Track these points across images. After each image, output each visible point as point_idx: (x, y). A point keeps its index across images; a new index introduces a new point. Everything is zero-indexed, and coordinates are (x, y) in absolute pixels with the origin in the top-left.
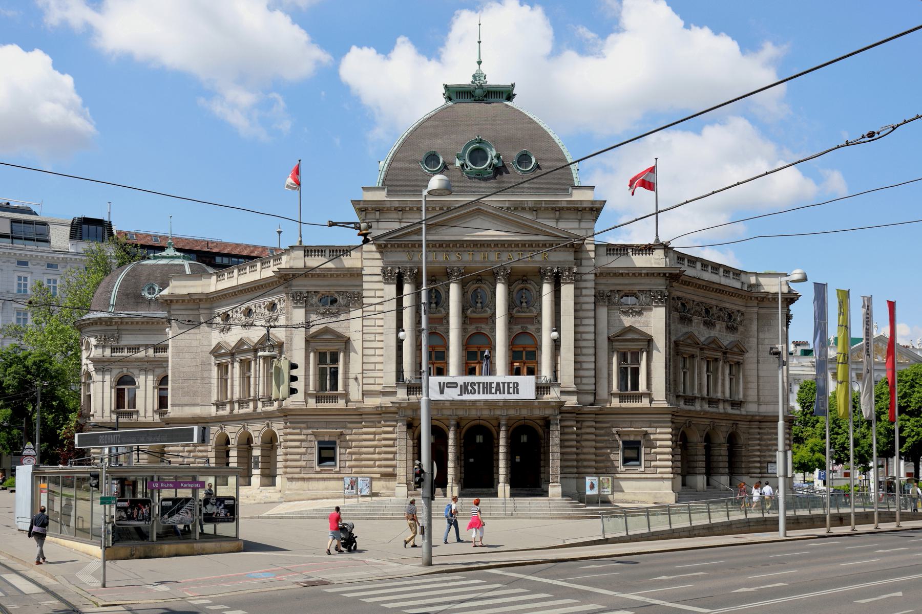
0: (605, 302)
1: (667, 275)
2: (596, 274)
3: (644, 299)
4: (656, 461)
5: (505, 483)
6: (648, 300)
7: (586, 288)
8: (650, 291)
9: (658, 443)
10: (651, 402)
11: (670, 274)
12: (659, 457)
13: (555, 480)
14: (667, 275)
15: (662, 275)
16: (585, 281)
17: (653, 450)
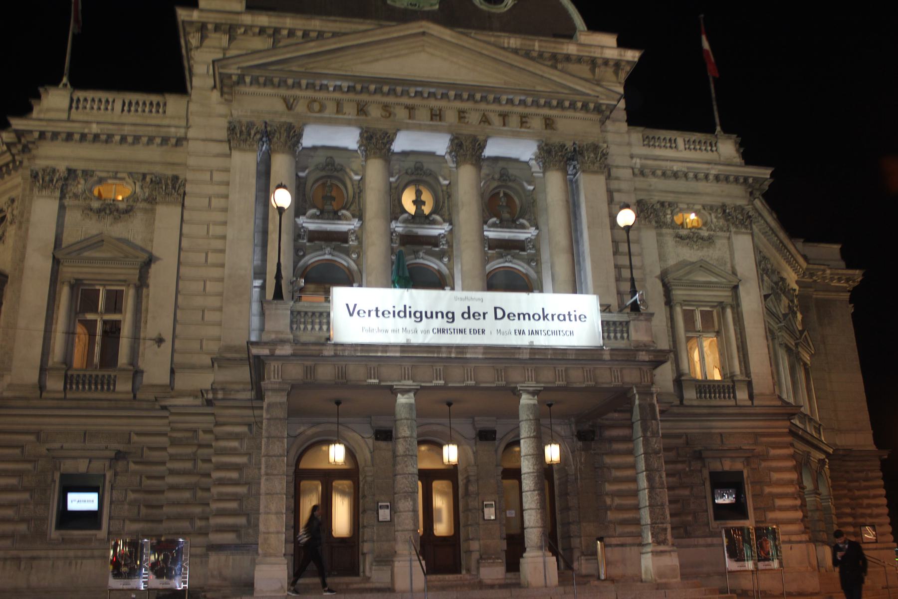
0: (650, 222)
1: (751, 180)
2: (633, 169)
3: (714, 220)
4: (773, 509)
5: (541, 548)
6: (722, 222)
7: (619, 191)
8: (723, 207)
9: (775, 476)
10: (751, 397)
11: (755, 179)
12: (779, 502)
13: (661, 537)
14: (751, 180)
15: (741, 180)
16: (617, 178)
17: (767, 490)
